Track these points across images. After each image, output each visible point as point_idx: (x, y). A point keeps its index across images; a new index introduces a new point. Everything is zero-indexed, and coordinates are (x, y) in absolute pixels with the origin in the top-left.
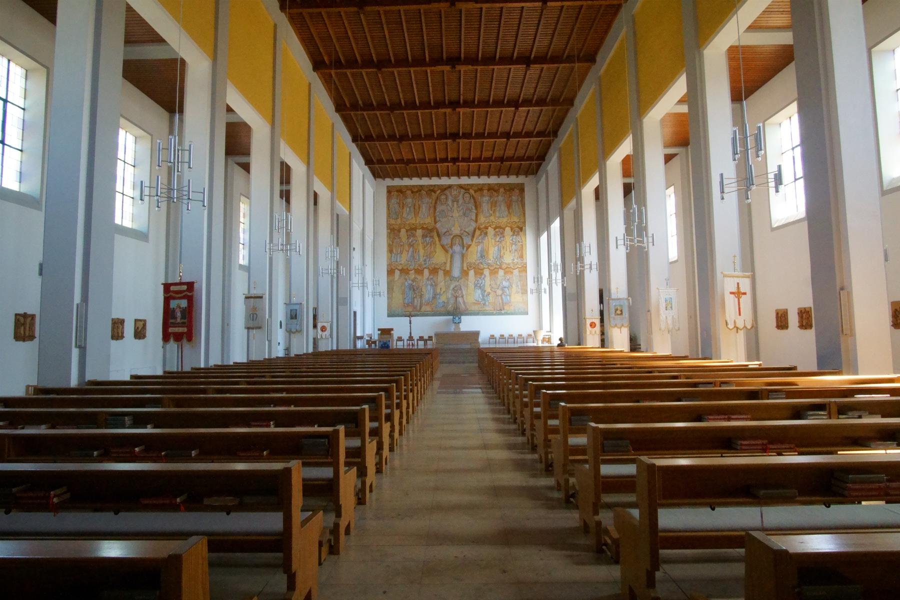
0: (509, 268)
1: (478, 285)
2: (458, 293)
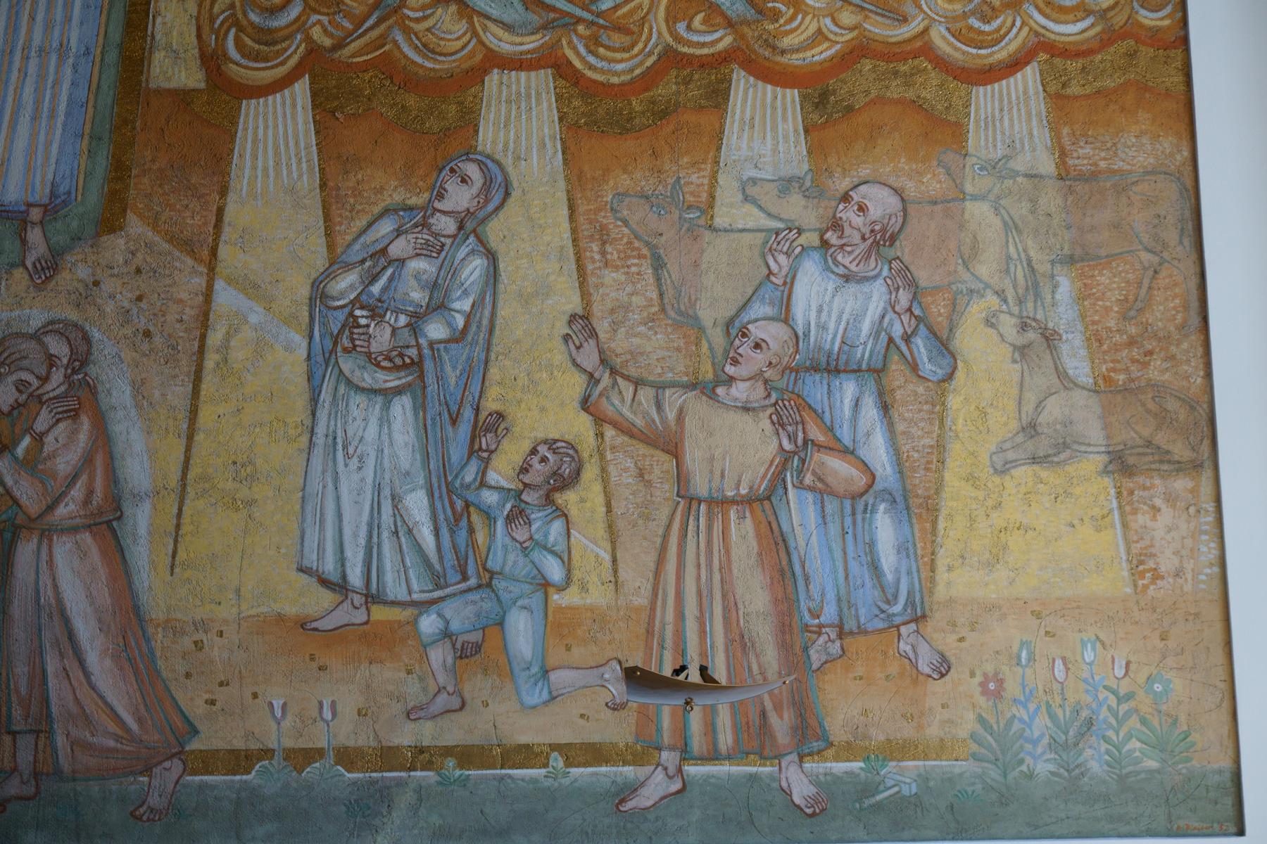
0: (891, 54)
1: (381, 339)
2: (31, 464)
